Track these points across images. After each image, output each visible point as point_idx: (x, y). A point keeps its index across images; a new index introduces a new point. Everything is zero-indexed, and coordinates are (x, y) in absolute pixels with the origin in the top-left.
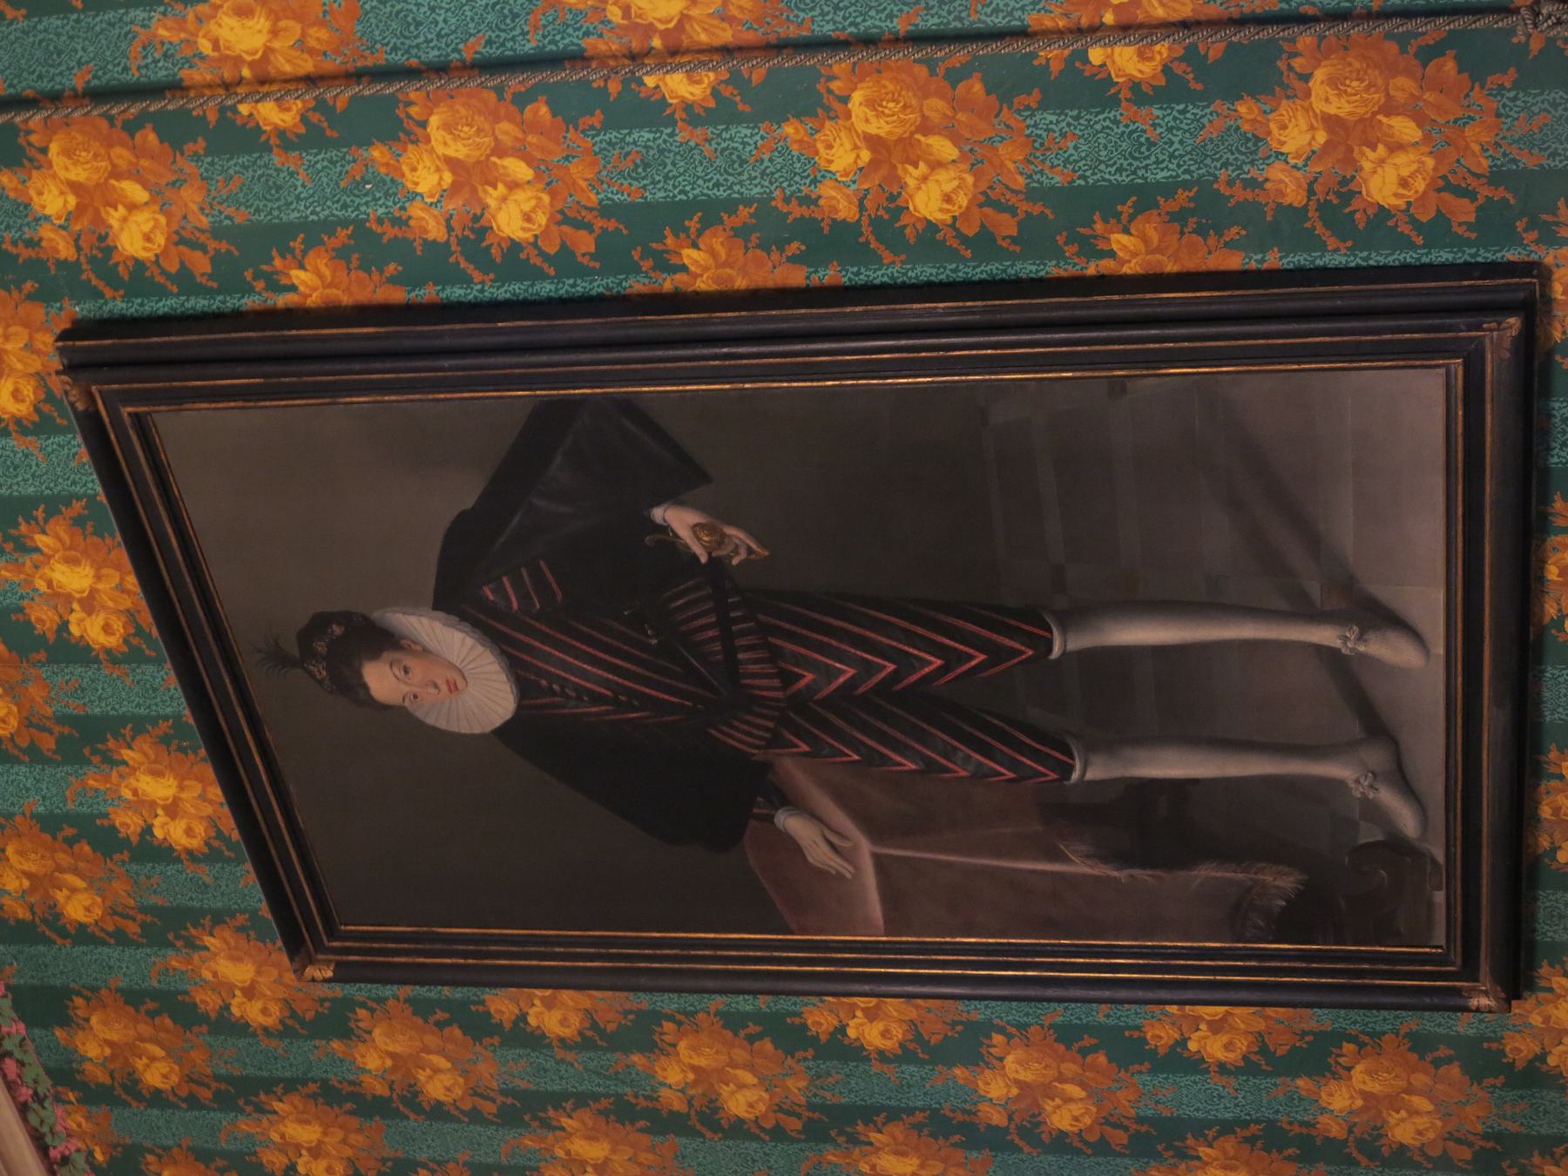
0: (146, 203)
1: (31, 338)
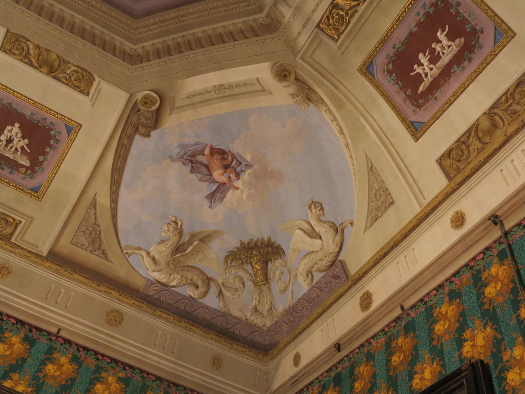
0: (522, 378)
1: (482, 353)
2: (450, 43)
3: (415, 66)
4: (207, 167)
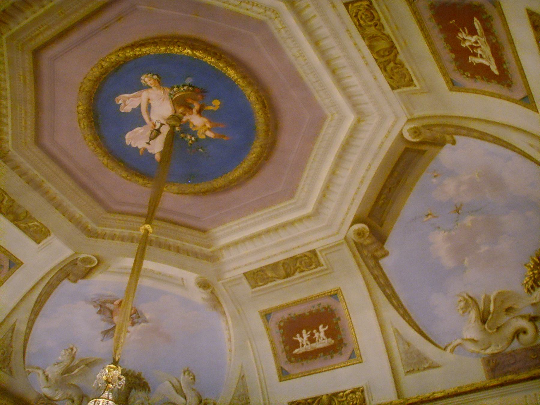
2: (325, 338)
3: (298, 335)
4: (112, 312)
